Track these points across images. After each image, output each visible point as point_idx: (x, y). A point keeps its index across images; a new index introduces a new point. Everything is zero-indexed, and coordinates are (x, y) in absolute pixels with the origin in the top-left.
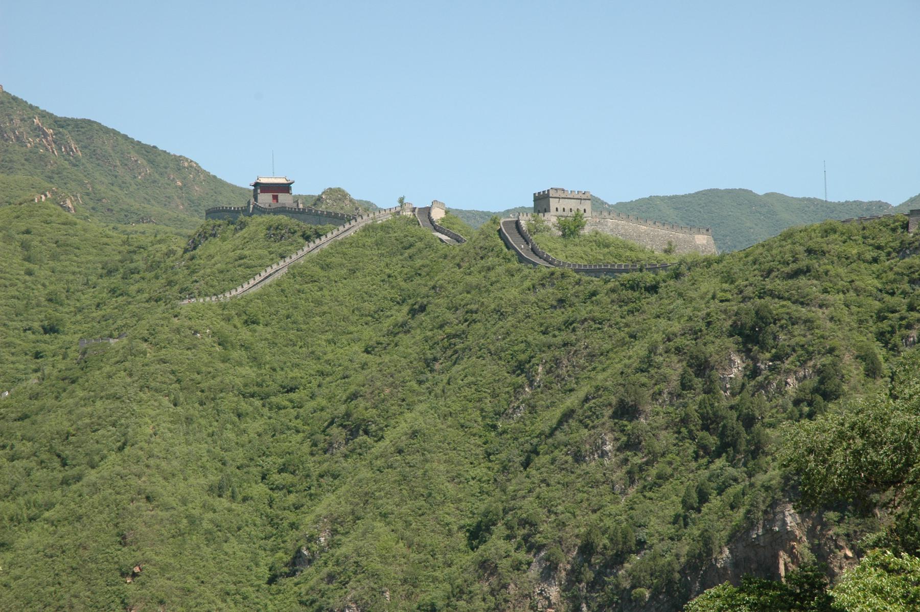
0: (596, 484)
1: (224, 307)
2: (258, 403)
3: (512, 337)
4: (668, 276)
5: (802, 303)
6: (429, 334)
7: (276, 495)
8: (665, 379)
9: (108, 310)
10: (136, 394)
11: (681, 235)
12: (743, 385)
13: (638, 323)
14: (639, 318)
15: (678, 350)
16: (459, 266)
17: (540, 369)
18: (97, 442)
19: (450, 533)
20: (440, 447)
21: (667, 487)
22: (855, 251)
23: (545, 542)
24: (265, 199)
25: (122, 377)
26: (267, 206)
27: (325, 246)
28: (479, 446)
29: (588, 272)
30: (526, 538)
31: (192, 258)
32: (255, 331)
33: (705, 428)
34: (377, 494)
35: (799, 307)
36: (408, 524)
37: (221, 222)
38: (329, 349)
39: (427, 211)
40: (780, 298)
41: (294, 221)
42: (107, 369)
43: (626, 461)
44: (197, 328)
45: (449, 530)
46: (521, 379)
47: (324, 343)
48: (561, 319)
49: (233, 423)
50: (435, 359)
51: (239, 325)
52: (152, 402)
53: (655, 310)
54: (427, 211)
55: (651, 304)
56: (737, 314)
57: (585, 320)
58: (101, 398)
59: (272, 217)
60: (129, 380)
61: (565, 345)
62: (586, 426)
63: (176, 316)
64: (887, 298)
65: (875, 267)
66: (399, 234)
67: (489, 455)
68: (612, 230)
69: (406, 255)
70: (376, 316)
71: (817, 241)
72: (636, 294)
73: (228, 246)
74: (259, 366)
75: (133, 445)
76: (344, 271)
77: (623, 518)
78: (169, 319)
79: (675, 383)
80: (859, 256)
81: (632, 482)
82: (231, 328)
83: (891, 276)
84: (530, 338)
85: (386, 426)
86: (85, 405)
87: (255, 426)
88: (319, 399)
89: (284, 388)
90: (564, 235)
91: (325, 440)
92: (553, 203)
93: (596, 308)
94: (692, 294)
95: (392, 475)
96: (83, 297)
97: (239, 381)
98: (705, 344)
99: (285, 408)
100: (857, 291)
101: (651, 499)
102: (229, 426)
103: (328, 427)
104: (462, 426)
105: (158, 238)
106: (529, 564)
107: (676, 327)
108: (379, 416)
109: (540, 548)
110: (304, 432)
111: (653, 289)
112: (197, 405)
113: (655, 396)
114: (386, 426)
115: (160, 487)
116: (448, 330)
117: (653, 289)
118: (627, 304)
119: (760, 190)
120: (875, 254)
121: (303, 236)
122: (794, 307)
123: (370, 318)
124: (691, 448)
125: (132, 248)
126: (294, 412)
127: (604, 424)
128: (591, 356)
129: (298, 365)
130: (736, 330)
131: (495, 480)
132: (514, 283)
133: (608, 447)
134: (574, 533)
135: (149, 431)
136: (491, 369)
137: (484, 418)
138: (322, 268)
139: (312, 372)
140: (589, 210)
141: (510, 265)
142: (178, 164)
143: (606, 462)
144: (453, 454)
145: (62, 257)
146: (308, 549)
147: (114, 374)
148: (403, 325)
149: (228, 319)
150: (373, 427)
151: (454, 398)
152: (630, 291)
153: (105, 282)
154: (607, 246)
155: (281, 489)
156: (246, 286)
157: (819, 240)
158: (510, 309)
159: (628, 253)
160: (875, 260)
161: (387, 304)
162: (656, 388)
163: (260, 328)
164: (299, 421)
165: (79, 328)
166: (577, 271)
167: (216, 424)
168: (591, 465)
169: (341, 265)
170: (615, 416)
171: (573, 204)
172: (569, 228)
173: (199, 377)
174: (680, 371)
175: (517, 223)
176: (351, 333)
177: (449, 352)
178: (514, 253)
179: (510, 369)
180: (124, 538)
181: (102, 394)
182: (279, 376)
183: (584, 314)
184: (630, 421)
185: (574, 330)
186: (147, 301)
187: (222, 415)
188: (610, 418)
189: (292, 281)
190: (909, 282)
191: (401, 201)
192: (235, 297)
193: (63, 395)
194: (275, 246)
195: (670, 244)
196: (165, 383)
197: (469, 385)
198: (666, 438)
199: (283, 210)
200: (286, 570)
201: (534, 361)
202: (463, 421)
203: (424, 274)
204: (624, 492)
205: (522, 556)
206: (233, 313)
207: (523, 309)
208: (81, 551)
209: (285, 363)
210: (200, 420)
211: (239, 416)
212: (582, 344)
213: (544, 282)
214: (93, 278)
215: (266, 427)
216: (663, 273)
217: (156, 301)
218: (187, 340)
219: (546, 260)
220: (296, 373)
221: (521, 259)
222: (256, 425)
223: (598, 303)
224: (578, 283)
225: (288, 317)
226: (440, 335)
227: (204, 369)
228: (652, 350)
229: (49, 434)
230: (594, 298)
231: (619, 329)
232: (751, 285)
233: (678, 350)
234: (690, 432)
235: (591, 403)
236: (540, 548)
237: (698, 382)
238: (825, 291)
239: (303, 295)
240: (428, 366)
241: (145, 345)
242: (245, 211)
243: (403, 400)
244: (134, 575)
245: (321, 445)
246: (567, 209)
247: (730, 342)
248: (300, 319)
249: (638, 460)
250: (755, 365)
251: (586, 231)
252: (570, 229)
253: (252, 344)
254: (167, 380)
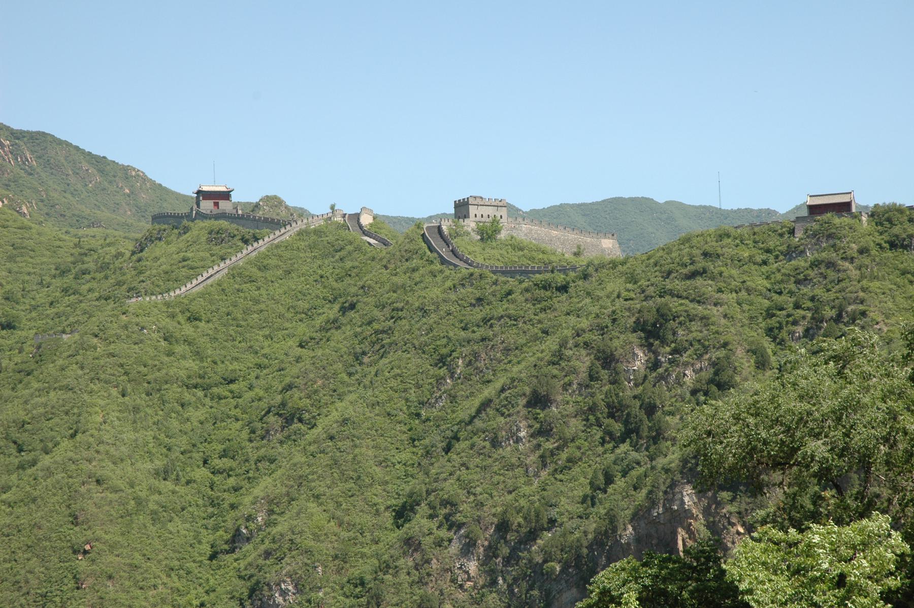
0: (511, 467)
1: (168, 305)
2: (200, 393)
3: (435, 333)
4: (576, 277)
5: (699, 302)
6: (359, 330)
7: (217, 478)
8: (575, 371)
9: (61, 308)
10: (87, 386)
11: (589, 240)
12: (646, 376)
13: (550, 320)
14: (551, 316)
15: (586, 345)
16: (386, 267)
17: (460, 361)
18: (52, 430)
19: (378, 513)
20: (368, 434)
21: (576, 470)
22: (746, 255)
23: (464, 520)
24: (207, 206)
25: (74, 370)
26: (208, 212)
27: (263, 249)
28: (404, 432)
29: (504, 273)
30: (447, 517)
31: (139, 260)
32: (198, 327)
33: (611, 415)
34: (310, 477)
35: (696, 306)
36: (339, 504)
37: (166, 226)
38: (266, 343)
39: (356, 217)
40: (679, 297)
41: (234, 226)
42: (60, 362)
43: (539, 446)
44: (142, 324)
45: (377, 510)
46: (443, 371)
47: (261, 338)
48: (479, 317)
49: (177, 413)
50: (364, 353)
51: (183, 322)
52: (102, 393)
53: (565, 308)
54: (356, 217)
55: (561, 302)
56: (640, 311)
57: (502, 317)
58: (55, 389)
59: (213, 222)
60: (80, 372)
61: (483, 340)
62: (503, 415)
63: (124, 313)
64: (776, 297)
65: (764, 269)
66: (331, 238)
67: (414, 440)
68: (526, 235)
69: (337, 257)
70: (308, 314)
71: (712, 245)
72: (548, 293)
73: (172, 248)
74: (202, 360)
75: (84, 432)
76: (280, 272)
77: (537, 497)
78: (117, 316)
79: (583, 375)
80: (751, 259)
81: (544, 465)
82: (175, 324)
83: (779, 277)
84: (451, 334)
85: (319, 415)
86: (39, 396)
87: (196, 415)
88: (257, 390)
89: (225, 379)
90: (482, 239)
91: (262, 428)
92: (472, 210)
93: (512, 306)
94: (598, 293)
95: (325, 460)
96: (37, 296)
97: (183, 374)
98: (611, 339)
99: (225, 398)
100: (749, 291)
101: (561, 481)
102: (173, 415)
103: (265, 415)
104: (389, 414)
105: (107, 241)
106: (450, 541)
107: (585, 323)
108: (312, 405)
109: (460, 526)
110: (242, 420)
111: (564, 289)
112: (143, 395)
113: (565, 387)
114: (319, 415)
115: (108, 470)
116: (376, 326)
117: (564, 289)
118: (540, 302)
119: (661, 199)
120: (764, 257)
121: (242, 239)
122: (691, 305)
123: (304, 315)
124: (598, 434)
125: (82, 251)
126: (233, 402)
127: (518, 412)
128: (507, 350)
129: (237, 359)
130: (640, 326)
131: (419, 464)
132: (437, 283)
133: (522, 434)
134: (492, 511)
135: (99, 419)
136: (415, 362)
137: (409, 407)
138: (260, 269)
139: (251, 365)
140: (505, 217)
141: (433, 267)
142: (126, 173)
143: (521, 447)
144: (380, 440)
145: (18, 259)
146: (246, 527)
147: (67, 367)
148: (335, 321)
149: (173, 316)
150: (306, 416)
151: (382, 389)
152: (542, 291)
153: (58, 282)
154: (522, 249)
155: (221, 473)
156: (189, 286)
157: (714, 244)
158: (433, 307)
159: (541, 256)
160: (765, 263)
161: (319, 302)
162: (567, 379)
163: (202, 324)
164: (238, 410)
165: (33, 324)
166: (494, 272)
167: (161, 413)
168: (507, 451)
169: (277, 267)
170: (529, 405)
171: (490, 211)
172: (487, 234)
173: (144, 370)
174: (588, 364)
175: (439, 228)
176: (286, 329)
177: (377, 347)
178: (436, 255)
179: (432, 362)
180: (76, 518)
181: (55, 386)
182: (220, 368)
183: (500, 311)
184: (543, 410)
185: (491, 326)
186: (97, 300)
187: (167, 405)
188: (524, 407)
189: (232, 281)
190: (795, 282)
191: (332, 207)
192: (179, 296)
193: (19, 386)
194: (216, 249)
195: (579, 247)
196: (114, 375)
197: (395, 377)
198: (575, 425)
199: (223, 216)
200: (226, 547)
201: (454, 354)
202: (388, 410)
203: (353, 274)
204: (537, 475)
205: (443, 533)
206: (178, 310)
207: (444, 307)
208: (35, 531)
209: (225, 357)
210: (147, 409)
211: (182, 405)
212: (498, 339)
213: (464, 282)
214: (47, 279)
215: (208, 415)
216: (572, 274)
217: (106, 299)
218: (134, 336)
219: (466, 262)
220: (236, 366)
221: (443, 261)
222: (198, 413)
223: (514, 301)
224: (495, 283)
225: (228, 314)
226: (368, 331)
227: (150, 362)
228: (563, 344)
229: (5, 422)
230: (510, 297)
231: (533, 325)
232: (652, 285)
233: (586, 345)
234: (597, 419)
235: (507, 393)
236: (460, 526)
237: (604, 374)
238: (720, 291)
239: (241, 294)
240: (357, 359)
241: (95, 340)
242: (188, 216)
243: (335, 391)
244: (85, 552)
245: (259, 432)
246: (485, 215)
247: (634, 338)
248: (239, 316)
249: (550, 445)
250: (656, 358)
251: (503, 235)
252: (488, 234)
253: (194, 339)
254: (116, 372)
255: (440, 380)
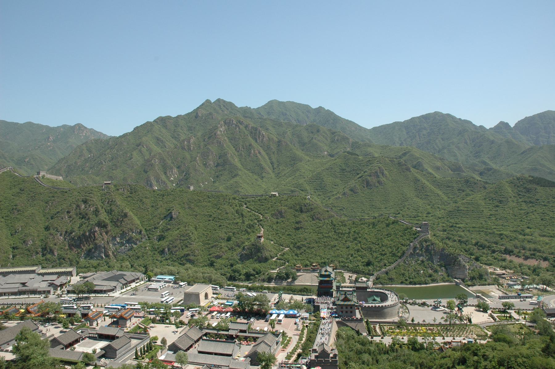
130: (83, 201)
134: (64, 230)
168: (64, 219)
198: (75, 216)
255: (47, 206)
